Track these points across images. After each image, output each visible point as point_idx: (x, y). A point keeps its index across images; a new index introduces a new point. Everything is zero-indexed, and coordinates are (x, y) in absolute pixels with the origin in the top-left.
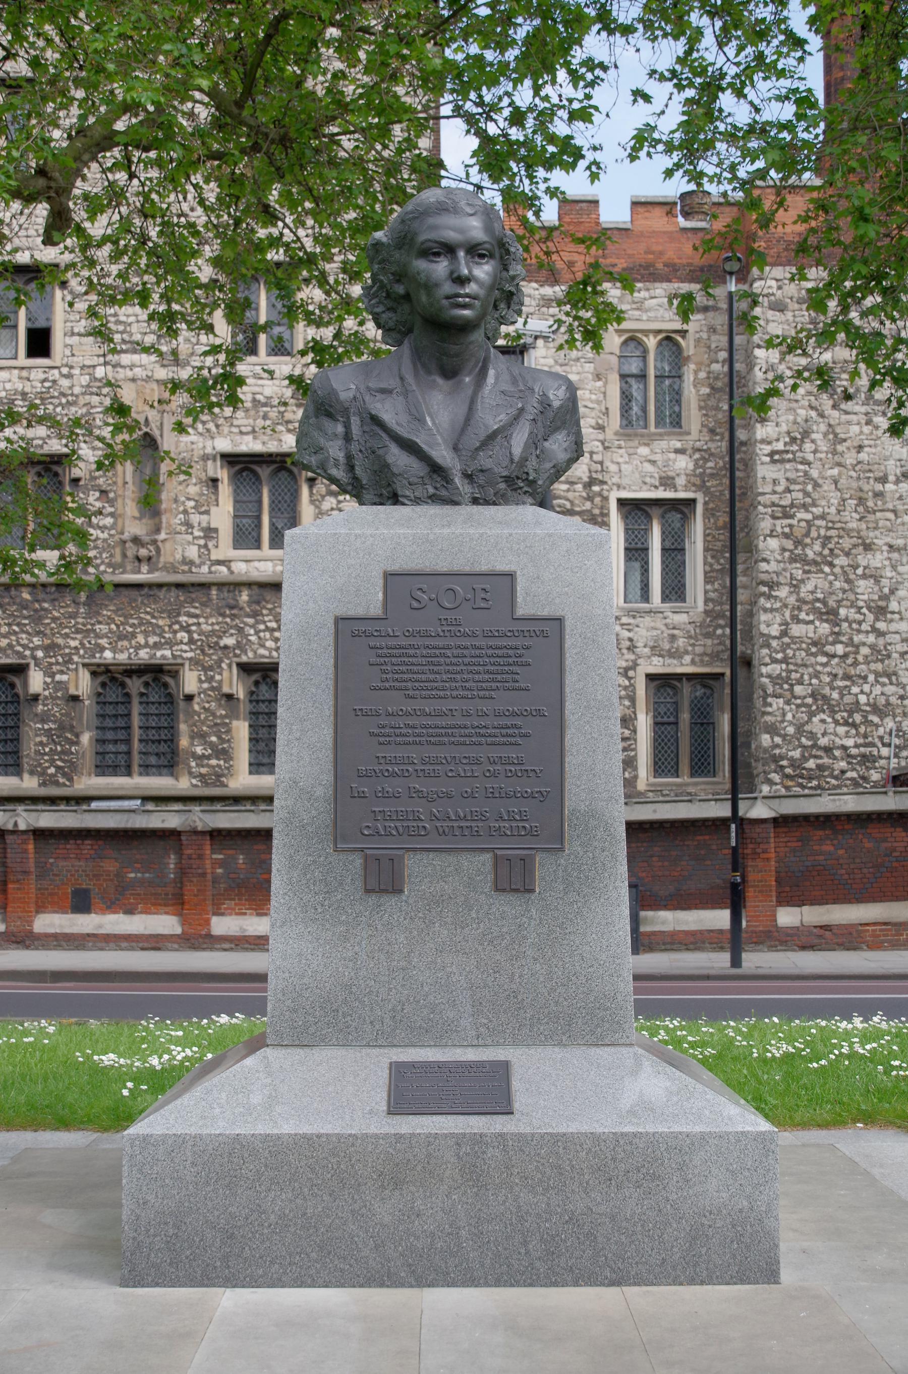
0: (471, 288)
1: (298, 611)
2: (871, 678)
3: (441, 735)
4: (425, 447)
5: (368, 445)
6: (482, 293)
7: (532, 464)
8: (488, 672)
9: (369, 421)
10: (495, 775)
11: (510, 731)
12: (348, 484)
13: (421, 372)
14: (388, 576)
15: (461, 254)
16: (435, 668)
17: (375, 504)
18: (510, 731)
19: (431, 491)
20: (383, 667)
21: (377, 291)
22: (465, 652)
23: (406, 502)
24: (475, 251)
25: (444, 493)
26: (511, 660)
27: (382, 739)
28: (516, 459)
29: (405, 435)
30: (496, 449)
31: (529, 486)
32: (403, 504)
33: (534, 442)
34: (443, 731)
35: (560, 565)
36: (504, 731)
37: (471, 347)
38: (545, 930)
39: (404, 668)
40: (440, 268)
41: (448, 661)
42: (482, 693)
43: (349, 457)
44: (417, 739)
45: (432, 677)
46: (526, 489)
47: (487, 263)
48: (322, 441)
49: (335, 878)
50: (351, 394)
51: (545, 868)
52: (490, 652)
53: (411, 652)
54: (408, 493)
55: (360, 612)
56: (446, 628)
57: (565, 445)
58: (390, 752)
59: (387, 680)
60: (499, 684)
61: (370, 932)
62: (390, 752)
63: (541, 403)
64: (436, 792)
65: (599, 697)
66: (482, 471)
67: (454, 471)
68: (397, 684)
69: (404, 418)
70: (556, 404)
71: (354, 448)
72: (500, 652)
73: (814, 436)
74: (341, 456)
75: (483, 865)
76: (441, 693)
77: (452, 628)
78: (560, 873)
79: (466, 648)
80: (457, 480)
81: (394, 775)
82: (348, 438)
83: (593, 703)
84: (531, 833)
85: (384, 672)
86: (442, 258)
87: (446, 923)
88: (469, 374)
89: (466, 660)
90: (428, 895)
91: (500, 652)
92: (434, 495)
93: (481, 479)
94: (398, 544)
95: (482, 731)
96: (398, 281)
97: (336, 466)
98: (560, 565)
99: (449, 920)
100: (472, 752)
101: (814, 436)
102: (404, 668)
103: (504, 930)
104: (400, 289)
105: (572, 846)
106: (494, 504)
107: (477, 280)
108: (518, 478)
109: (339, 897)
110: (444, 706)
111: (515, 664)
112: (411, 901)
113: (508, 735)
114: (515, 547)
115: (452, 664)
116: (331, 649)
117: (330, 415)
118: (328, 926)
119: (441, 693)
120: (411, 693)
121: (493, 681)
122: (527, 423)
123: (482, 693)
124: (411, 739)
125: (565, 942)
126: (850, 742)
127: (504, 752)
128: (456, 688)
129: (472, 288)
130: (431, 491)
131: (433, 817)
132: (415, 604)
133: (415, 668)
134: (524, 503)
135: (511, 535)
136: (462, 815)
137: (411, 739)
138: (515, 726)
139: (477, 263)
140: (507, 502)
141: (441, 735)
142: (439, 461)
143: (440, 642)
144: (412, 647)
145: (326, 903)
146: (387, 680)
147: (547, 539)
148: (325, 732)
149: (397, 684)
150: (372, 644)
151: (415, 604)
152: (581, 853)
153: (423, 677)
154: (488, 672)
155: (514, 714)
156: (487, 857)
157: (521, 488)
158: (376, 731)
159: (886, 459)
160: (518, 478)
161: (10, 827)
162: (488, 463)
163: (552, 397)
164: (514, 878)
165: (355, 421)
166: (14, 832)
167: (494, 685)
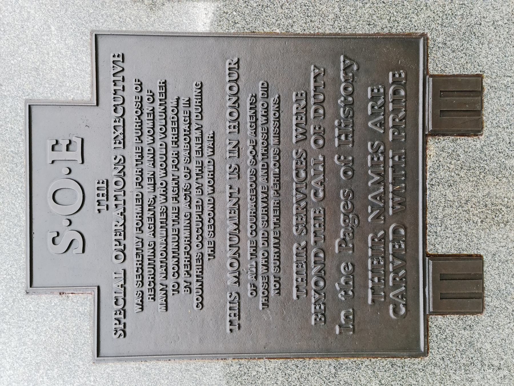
3: (266, 208)
10: (320, 134)
11: (260, 111)
16: (171, 216)
18: (260, 111)
20: (170, 289)
22: (146, 176)
26: (158, 110)
27: (273, 293)
34: (260, 205)
36: (261, 120)
39: (171, 262)
41: (160, 199)
42: (207, 151)
44: (272, 241)
45: (183, 222)
49: (463, 352)
52: (147, 139)
53: (147, 252)
56: (112, 202)
60: (194, 126)
64: (346, 215)
68: (194, 272)
72: (147, 125)
76: (207, 208)
77: (112, 194)
81: (321, 275)
89: (159, 173)
91: (147, 125)
95: (260, 149)
102: (171, 262)
109: (488, 346)
110: (224, 203)
111: (164, 103)
113: (266, 115)
119: (207, 208)
120: (206, 251)
121: (188, 134)
123: (207, 151)
124: (272, 250)
128: (200, 188)
133: (171, 246)
136: (377, 178)
137: (272, 250)
141: (266, 208)
143: (132, 210)
145: (496, 363)
149: (194, 272)
153: (184, 234)
156: (431, 141)
158: (261, 300)
164: (460, 105)
167: (195, 134)
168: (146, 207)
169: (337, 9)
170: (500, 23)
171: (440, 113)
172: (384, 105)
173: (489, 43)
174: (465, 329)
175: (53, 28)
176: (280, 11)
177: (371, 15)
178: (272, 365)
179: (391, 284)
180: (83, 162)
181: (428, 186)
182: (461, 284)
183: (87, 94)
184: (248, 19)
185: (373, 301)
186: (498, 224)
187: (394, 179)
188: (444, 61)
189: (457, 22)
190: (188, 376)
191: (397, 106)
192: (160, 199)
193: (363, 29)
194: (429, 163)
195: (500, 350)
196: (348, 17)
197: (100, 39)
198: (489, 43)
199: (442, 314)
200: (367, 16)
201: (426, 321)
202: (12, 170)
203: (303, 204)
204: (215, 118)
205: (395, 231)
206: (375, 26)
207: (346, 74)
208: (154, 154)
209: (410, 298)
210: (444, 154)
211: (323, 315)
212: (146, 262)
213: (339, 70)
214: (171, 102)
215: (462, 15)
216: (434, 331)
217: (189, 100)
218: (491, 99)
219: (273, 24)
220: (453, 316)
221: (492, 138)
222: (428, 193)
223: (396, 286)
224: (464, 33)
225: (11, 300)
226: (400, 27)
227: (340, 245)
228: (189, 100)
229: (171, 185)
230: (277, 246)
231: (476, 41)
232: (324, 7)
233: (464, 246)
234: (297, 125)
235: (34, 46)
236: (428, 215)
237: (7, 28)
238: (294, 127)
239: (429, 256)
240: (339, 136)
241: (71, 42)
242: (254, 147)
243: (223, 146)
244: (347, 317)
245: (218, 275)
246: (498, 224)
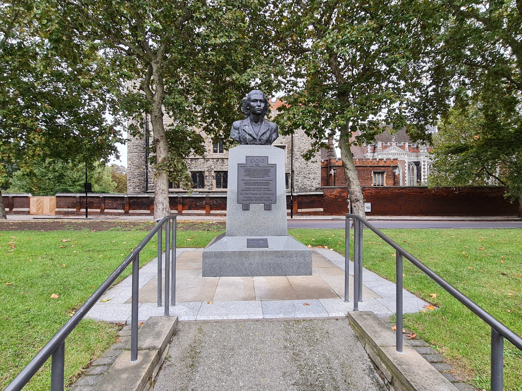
7: (270, 138)
33: (271, 135)
55: (242, 163)
58: (248, 187)
62: (248, 187)
82: (239, 133)
100: (261, 187)
105: (278, 202)
127: (266, 187)
164: (268, 208)
183: (269, 163)
188: (273, 205)
204: (266, 178)
243: (263, 179)
245: (248, 178)
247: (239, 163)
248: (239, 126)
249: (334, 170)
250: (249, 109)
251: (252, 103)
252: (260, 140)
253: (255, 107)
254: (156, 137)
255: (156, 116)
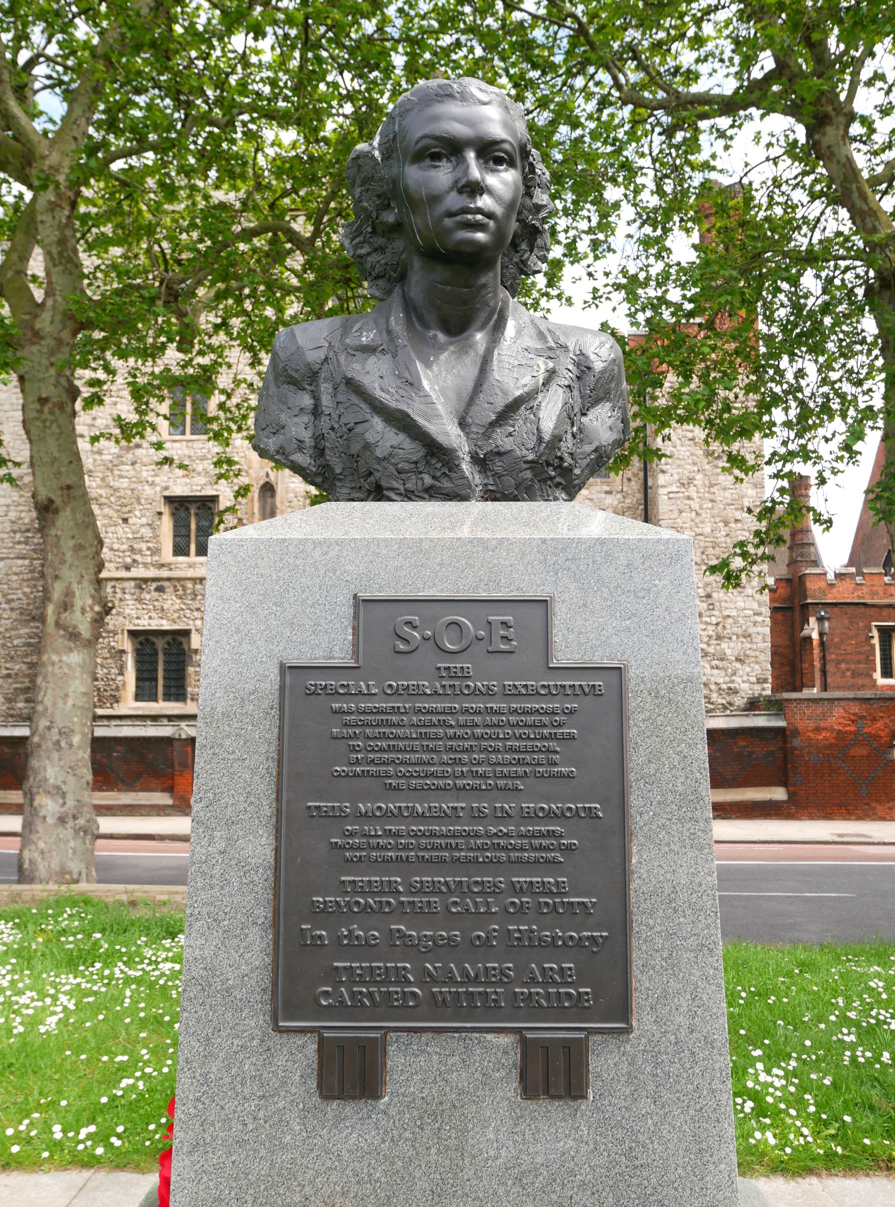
0: (485, 202)
1: (226, 655)
2: (734, 638)
3: (440, 848)
4: (421, 421)
5: (343, 420)
6: (498, 210)
7: (568, 444)
8: (511, 750)
9: (343, 387)
10: (521, 909)
11: (545, 842)
12: (317, 474)
13: (417, 325)
14: (360, 603)
15: (471, 155)
17: (353, 500)
18: (545, 842)
19: (428, 480)
21: (360, 227)
23: (395, 497)
24: (491, 152)
25: (446, 484)
28: (547, 437)
29: (393, 404)
30: (520, 424)
31: (561, 475)
32: (390, 500)
33: (569, 416)
34: (443, 842)
35: (618, 586)
36: (535, 842)
37: (483, 292)
38: (603, 1161)
40: (442, 176)
41: (451, 732)
42: (501, 783)
43: (319, 438)
46: (558, 479)
47: (506, 170)
48: (283, 418)
50: (321, 354)
51: (605, 1062)
54: (395, 484)
57: (610, 422)
59: (358, 762)
61: (329, 1164)
63: (577, 365)
64: (433, 938)
65: (680, 788)
66: (499, 454)
67: (460, 454)
69: (391, 384)
70: (598, 366)
71: (324, 423)
72: (530, 719)
73: (695, 482)
74: (306, 436)
75: (505, 1053)
78: (625, 1067)
79: (478, 712)
80: (466, 467)
82: (316, 412)
83: (670, 797)
84: (578, 1009)
85: (353, 749)
86: (443, 163)
87: (447, 1148)
88: (482, 328)
89: (478, 731)
90: (419, 1102)
91: (530, 719)
92: (432, 487)
93: (498, 465)
94: (377, 555)
96: (388, 206)
97: (300, 449)
98: (618, 586)
99: (452, 1143)
101: (695, 482)
103: (539, 1160)
104: (390, 218)
105: (642, 1020)
106: (515, 499)
107: (489, 191)
108: (548, 464)
109: (281, 1105)
111: (552, 737)
112: (393, 1112)
113: (541, 848)
114: (551, 559)
115: (455, 737)
116: (275, 712)
117: (294, 383)
118: (263, 1153)
121: (520, 763)
122: (560, 390)
123: (501, 783)
125: (635, 1181)
126: (721, 681)
129: (485, 202)
130: (428, 480)
131: (426, 979)
132: (402, 647)
134: (556, 499)
135: (544, 541)
138: (551, 834)
139: (493, 171)
140: (532, 498)
141: (440, 848)
142: (441, 439)
144: (396, 711)
145: (261, 1114)
146: (358, 762)
147: (598, 547)
148: (264, 841)
150: (335, 706)
151: (402, 647)
152: (657, 1036)
153: (414, 757)
154: (511, 750)
155: (551, 816)
157: (551, 478)
159: (743, 497)
160: (548, 464)
161: (177, 736)
162: (507, 444)
163: (593, 357)
165: (325, 388)
166: (179, 740)
167: (520, 770)
168: (442, 718)
169: (659, 929)
170: (650, 1122)
171: (546, 1047)
172: (554, 982)
173: (627, 1108)
174: (302, 1076)
175: (628, 622)
176: (656, 864)
177: (653, 968)
178: (268, 852)
179: (355, 989)
180: (489, 652)
181: (463, 1034)
182: (351, 1074)
184: (646, 829)
185: (337, 968)
186: (421, 1118)
187: (472, 993)
189: (649, 1069)
190: (261, 759)
191: (553, 998)
192: (451, 732)
193: (637, 957)
194: (489, 1037)
195: (276, 1119)
196: (651, 941)
197: (617, 672)
198: (627, 1108)
199: (320, 1050)
200: (653, 963)
201: (311, 1030)
202: (481, 580)
203: (444, 889)
205: (414, 994)
206: (642, 972)
207: (588, 938)
208: (499, 726)
209: (339, 1010)
210: (499, 1054)
211: (323, 911)
212: (385, 717)
213: (592, 931)
214: (552, 744)
215: (657, 1076)
216: (300, 1040)
217: (556, 764)
218: (563, 1110)
219: (642, 856)
220: (316, 1062)
221: (518, 1111)
222: (456, 1035)
223: (353, 995)
224: (636, 1077)
225: (348, 578)
226: (637, 999)
227: (399, 930)
228: (556, 764)
229: (467, 744)
230: (399, 859)
231: (627, 1093)
232: (661, 913)
233: (395, 1077)
234: (531, 882)
235: (609, 603)
236: (430, 1035)
237: (627, 576)
238: (528, 879)
239: (386, 1034)
240: (519, 931)
241: (614, 640)
242: (506, 834)
244: (320, 937)
246: (421, 1118)
247: (295, 658)
248: (314, 357)
249: (820, 620)
250: (398, 227)
251: (414, 174)
252: (481, 462)
253: (435, 199)
254: (44, 494)
255: (43, 401)
